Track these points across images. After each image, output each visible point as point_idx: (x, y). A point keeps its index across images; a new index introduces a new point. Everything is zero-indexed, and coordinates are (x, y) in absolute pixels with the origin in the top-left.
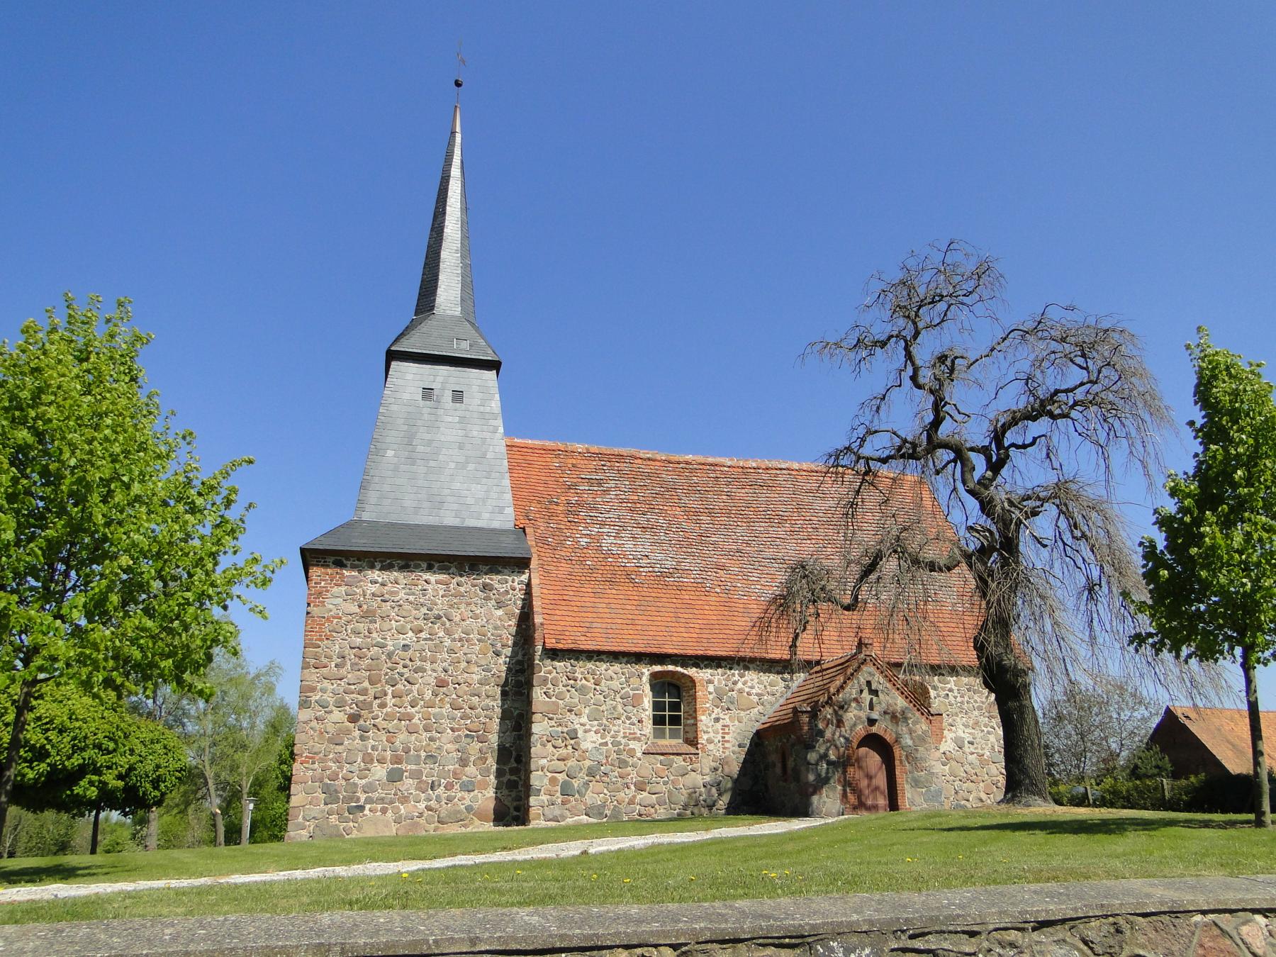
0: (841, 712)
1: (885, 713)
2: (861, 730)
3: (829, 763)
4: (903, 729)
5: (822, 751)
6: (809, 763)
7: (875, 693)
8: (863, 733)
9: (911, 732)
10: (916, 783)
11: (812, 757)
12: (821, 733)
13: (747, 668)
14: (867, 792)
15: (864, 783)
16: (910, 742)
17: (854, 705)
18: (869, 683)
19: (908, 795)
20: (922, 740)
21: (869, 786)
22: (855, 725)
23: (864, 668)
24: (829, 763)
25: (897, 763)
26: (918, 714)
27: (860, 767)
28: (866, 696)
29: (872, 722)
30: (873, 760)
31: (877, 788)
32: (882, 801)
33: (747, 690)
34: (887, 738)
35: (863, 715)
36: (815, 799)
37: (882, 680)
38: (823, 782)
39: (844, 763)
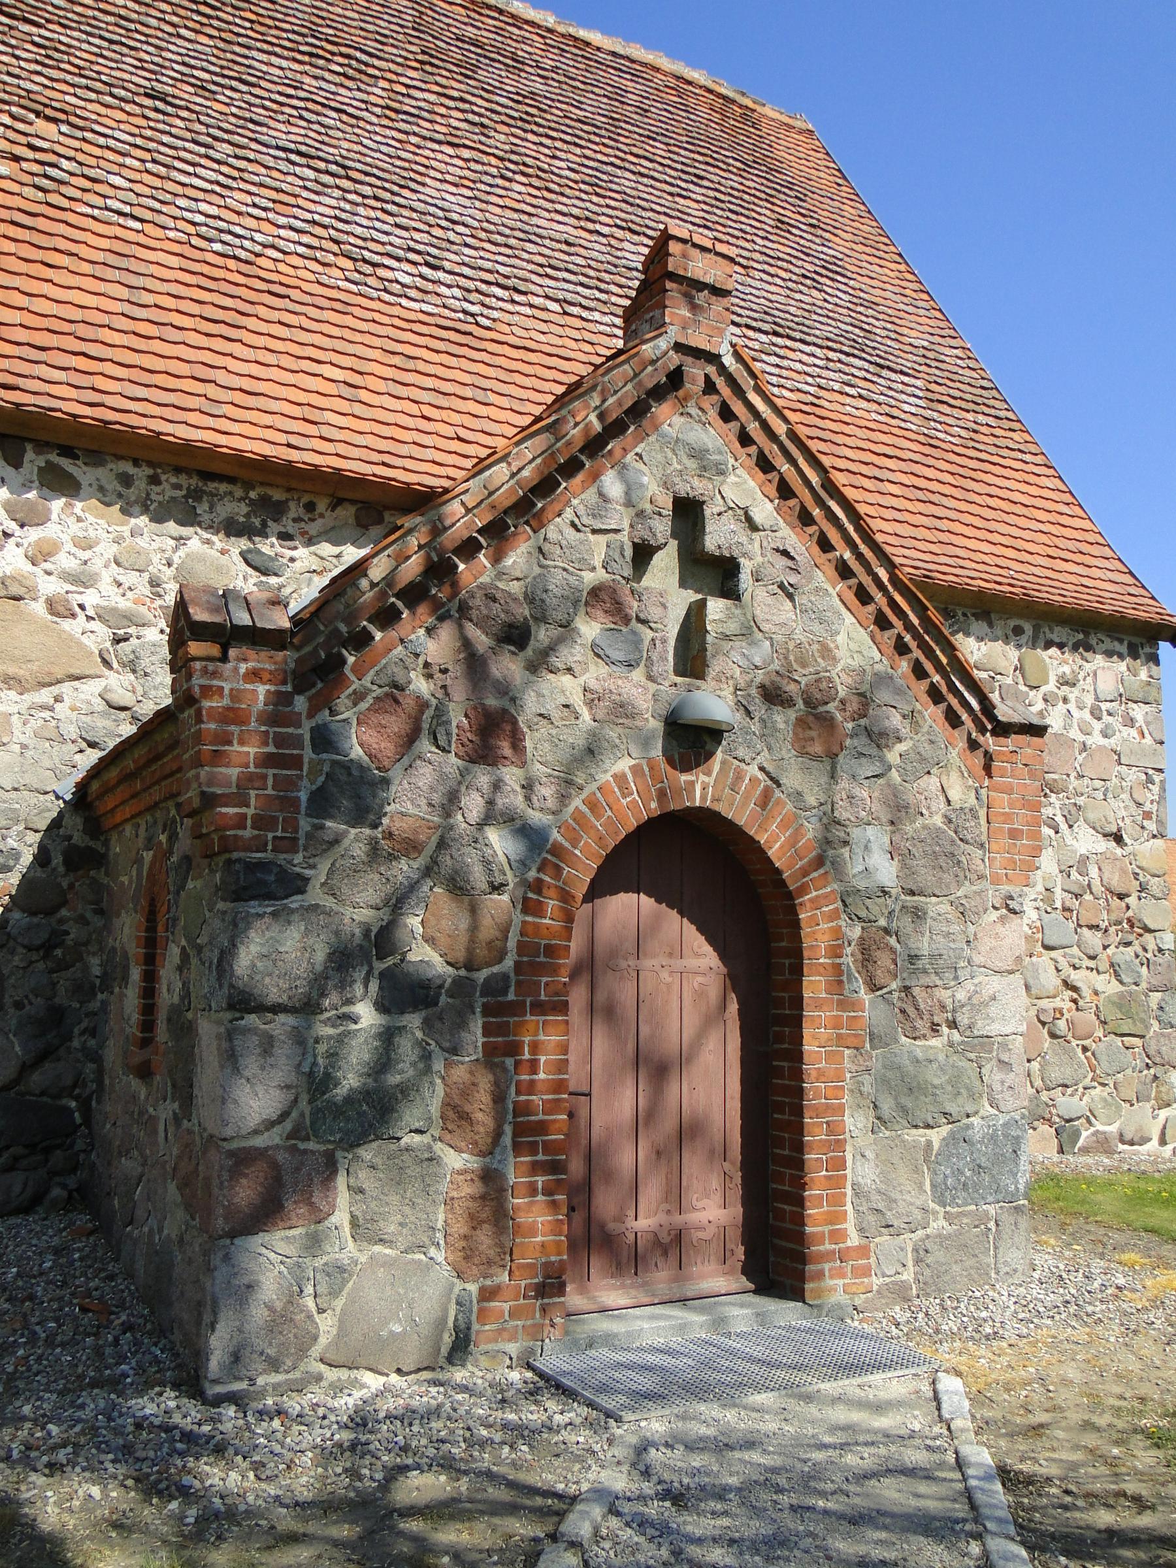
0: (508, 666)
1: (773, 695)
2: (626, 785)
3: (404, 993)
4: (859, 795)
5: (359, 909)
6: (244, 1002)
7: (717, 574)
8: (634, 808)
9: (899, 811)
10: (904, 1099)
11: (275, 952)
12: (355, 792)
13: (59, 483)
14: (625, 1159)
15: (616, 1106)
16: (886, 872)
17: (590, 629)
18: (688, 513)
19: (861, 1170)
20: (947, 853)
21: (643, 1120)
22: (591, 751)
23: (669, 419)
24: (404, 993)
25: (814, 986)
26: (932, 714)
27: (603, 1011)
28: (665, 590)
29: (691, 740)
30: (680, 968)
31: (688, 1132)
32: (713, 1208)
33: (50, 586)
34: (776, 842)
35: (647, 692)
36: (272, 1257)
37: (765, 511)
38: (342, 1123)
39: (503, 996)
